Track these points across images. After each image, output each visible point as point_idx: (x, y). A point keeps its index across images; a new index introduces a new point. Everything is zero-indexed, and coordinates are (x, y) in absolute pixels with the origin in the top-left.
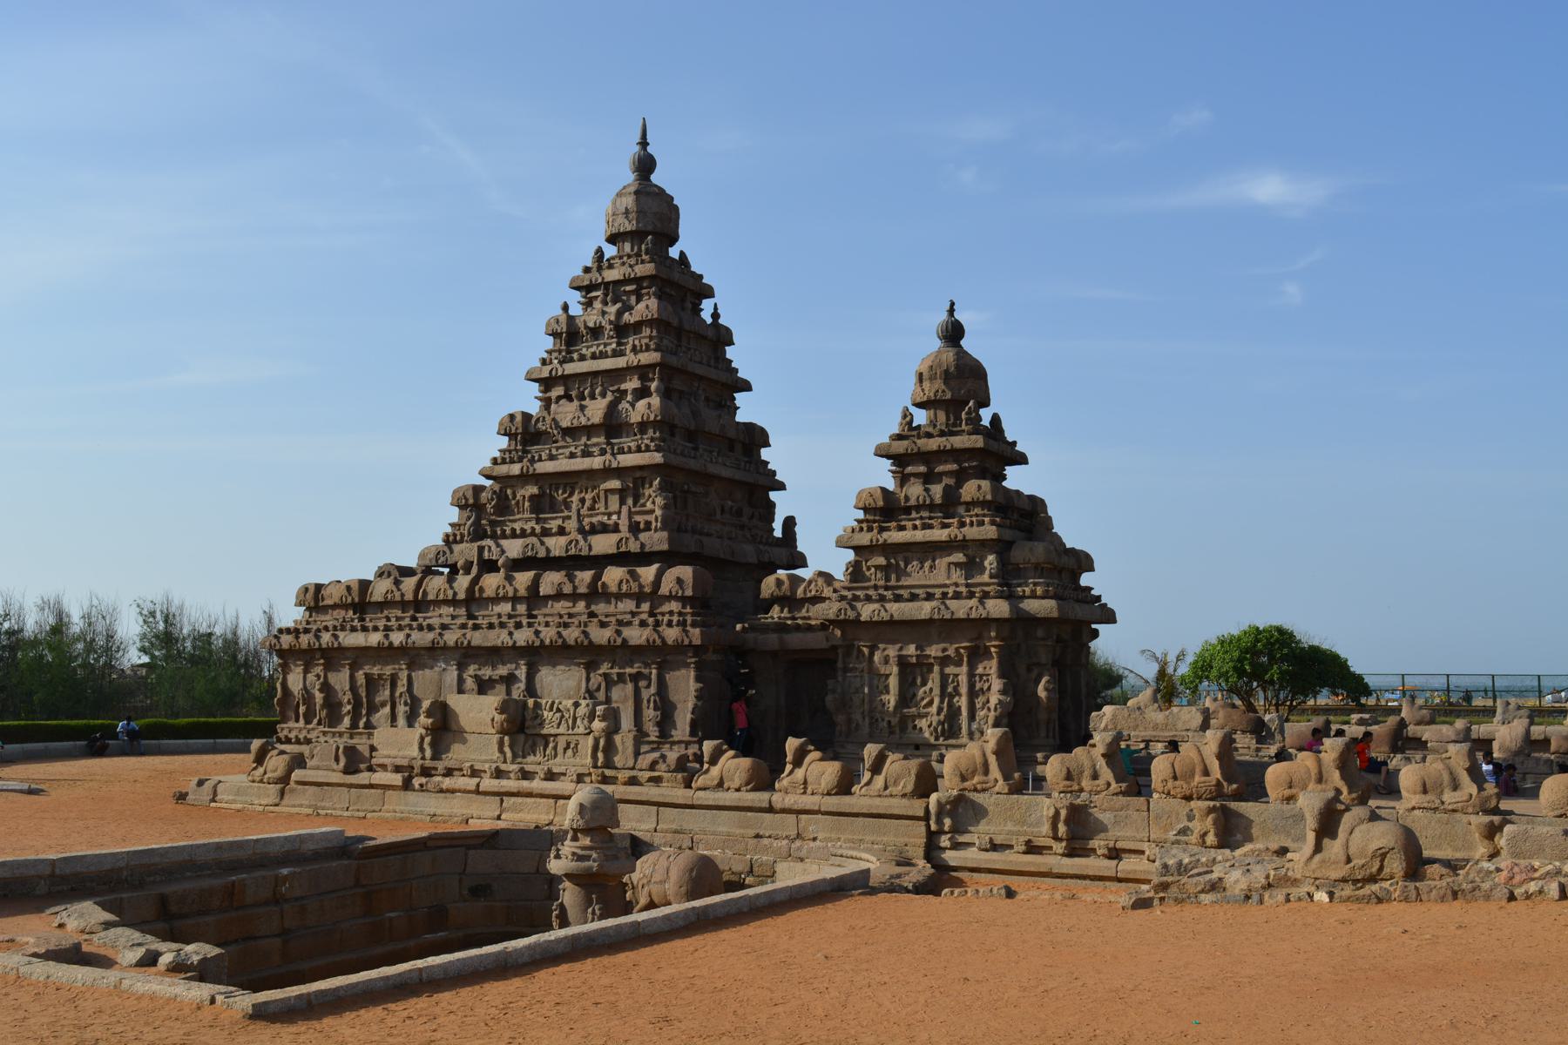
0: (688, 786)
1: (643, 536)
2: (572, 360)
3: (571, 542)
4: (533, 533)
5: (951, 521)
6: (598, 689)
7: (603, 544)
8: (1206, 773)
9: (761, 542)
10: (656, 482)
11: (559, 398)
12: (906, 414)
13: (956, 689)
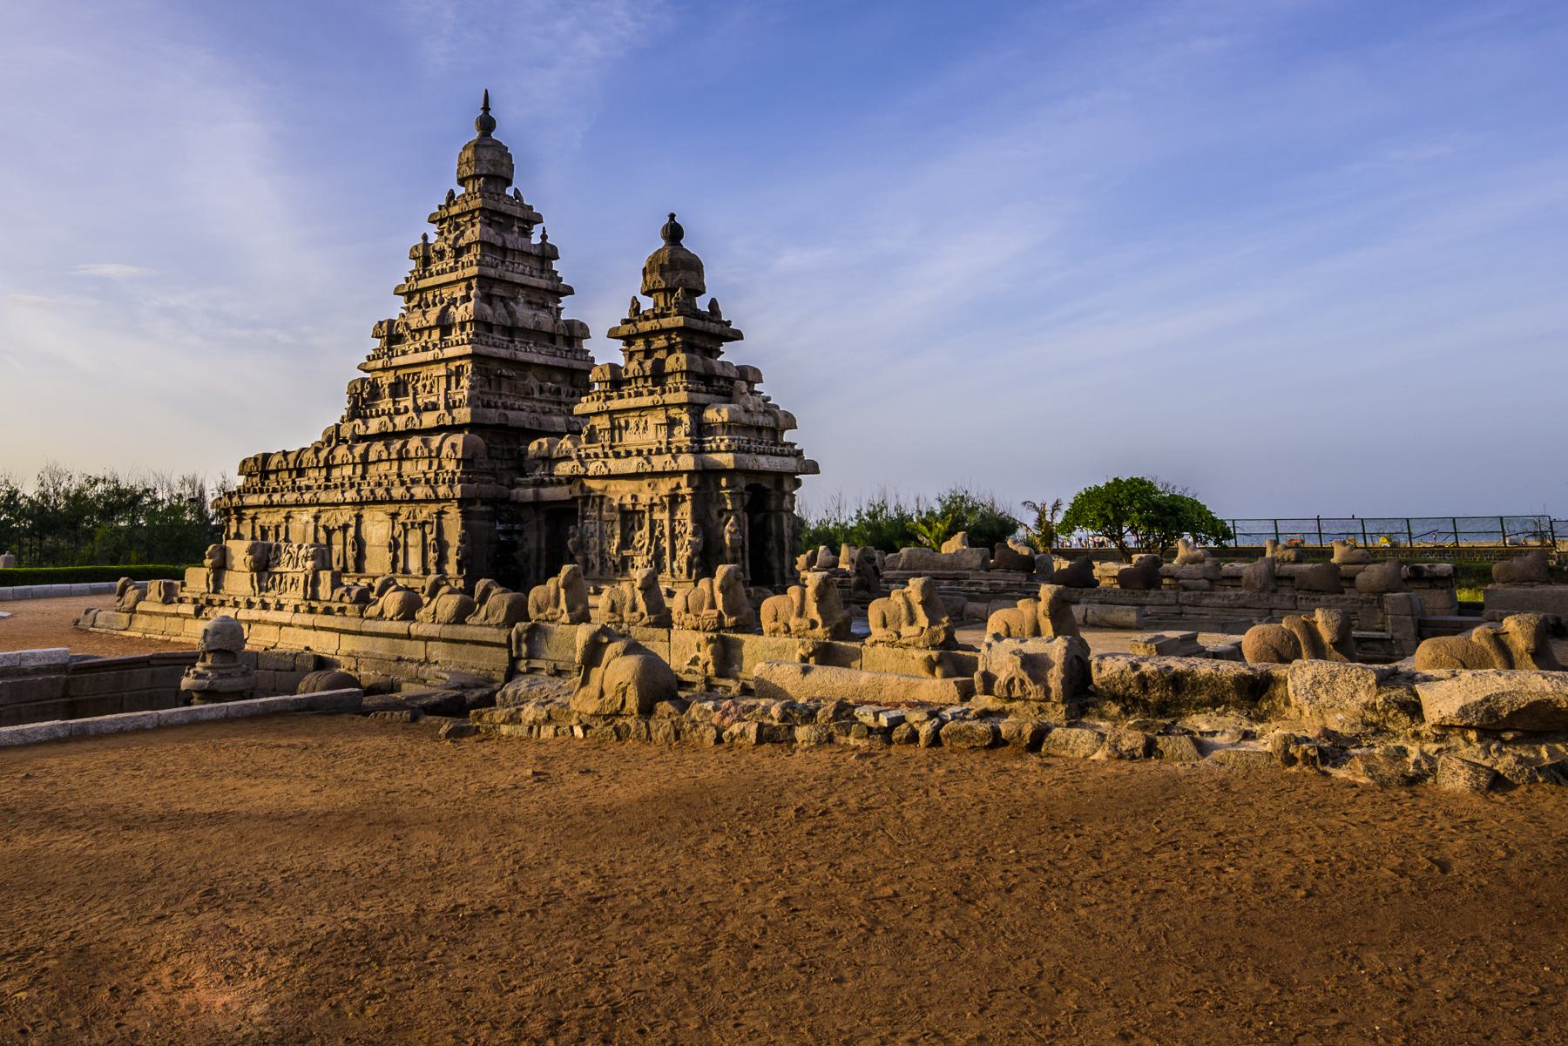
0: (361, 616)
1: (455, 412)
2: (425, 277)
6: (400, 536)
7: (429, 420)
8: (713, 606)
10: (470, 367)
11: (414, 307)
13: (662, 533)
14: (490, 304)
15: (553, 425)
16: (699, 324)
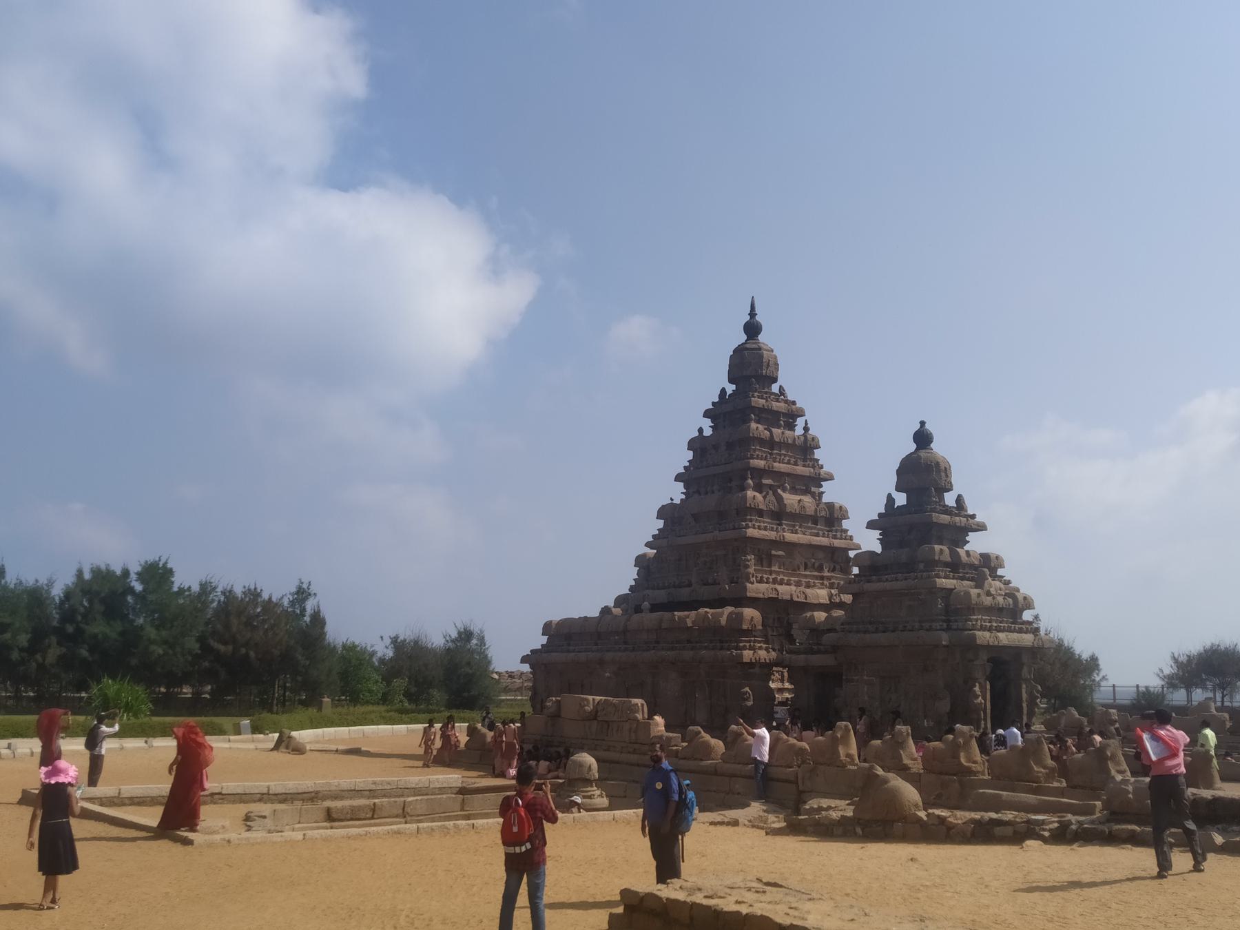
3: (693, 590)
4: (674, 586)
11: (694, 492)
12: (890, 497)
14: (760, 493)
15: (818, 596)
16: (945, 519)
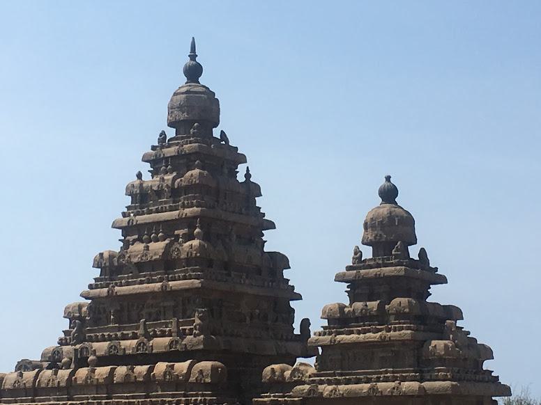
3: (140, 344)
4: (117, 338)
5: (382, 327)
7: (161, 343)
9: (281, 339)
11: (134, 241)
12: (358, 252)
